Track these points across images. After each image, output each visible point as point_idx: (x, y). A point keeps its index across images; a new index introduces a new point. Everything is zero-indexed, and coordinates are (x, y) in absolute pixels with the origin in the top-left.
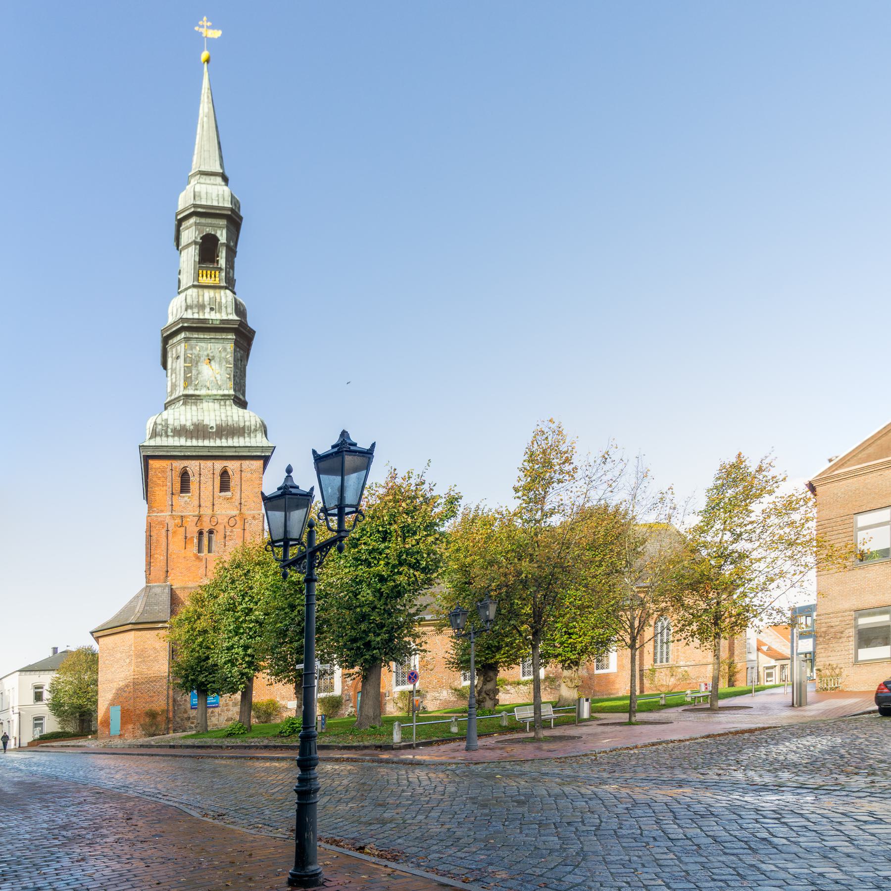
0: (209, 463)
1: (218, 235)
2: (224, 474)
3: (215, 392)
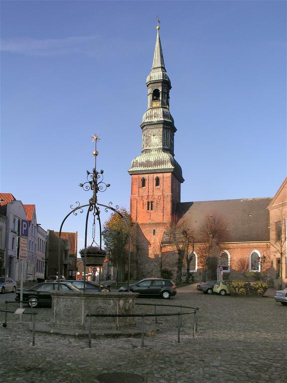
0: (152, 175)
2: (158, 180)
3: (156, 147)
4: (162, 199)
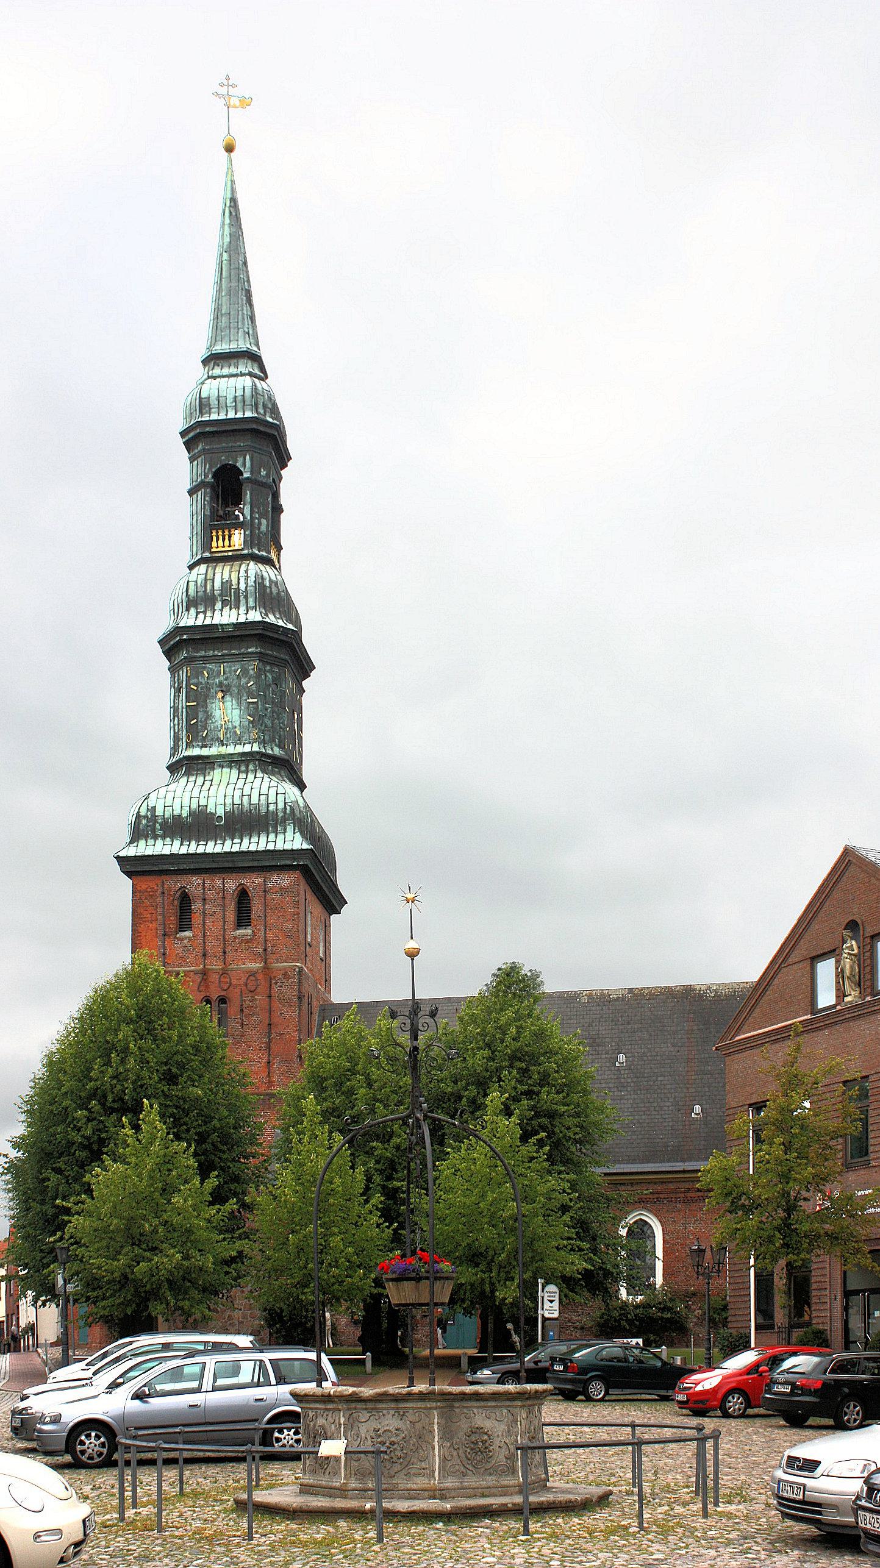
1: (239, 465)
2: (243, 897)
3: (231, 749)
4: (263, 988)
